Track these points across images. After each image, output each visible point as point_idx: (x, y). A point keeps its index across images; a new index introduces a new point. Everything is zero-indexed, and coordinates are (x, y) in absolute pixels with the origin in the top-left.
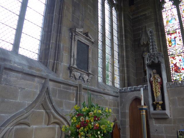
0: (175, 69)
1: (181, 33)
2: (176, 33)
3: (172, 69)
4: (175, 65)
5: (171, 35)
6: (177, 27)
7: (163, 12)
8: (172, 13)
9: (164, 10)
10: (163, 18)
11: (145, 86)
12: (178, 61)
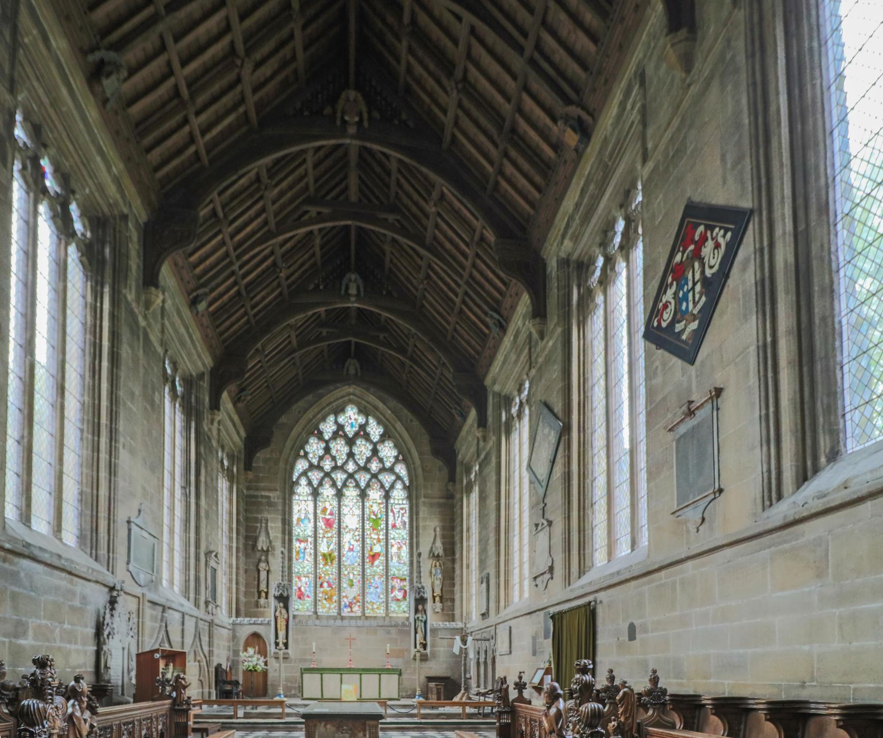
2: (307, 541)
4: (300, 589)
6: (310, 534)
9: (297, 497)
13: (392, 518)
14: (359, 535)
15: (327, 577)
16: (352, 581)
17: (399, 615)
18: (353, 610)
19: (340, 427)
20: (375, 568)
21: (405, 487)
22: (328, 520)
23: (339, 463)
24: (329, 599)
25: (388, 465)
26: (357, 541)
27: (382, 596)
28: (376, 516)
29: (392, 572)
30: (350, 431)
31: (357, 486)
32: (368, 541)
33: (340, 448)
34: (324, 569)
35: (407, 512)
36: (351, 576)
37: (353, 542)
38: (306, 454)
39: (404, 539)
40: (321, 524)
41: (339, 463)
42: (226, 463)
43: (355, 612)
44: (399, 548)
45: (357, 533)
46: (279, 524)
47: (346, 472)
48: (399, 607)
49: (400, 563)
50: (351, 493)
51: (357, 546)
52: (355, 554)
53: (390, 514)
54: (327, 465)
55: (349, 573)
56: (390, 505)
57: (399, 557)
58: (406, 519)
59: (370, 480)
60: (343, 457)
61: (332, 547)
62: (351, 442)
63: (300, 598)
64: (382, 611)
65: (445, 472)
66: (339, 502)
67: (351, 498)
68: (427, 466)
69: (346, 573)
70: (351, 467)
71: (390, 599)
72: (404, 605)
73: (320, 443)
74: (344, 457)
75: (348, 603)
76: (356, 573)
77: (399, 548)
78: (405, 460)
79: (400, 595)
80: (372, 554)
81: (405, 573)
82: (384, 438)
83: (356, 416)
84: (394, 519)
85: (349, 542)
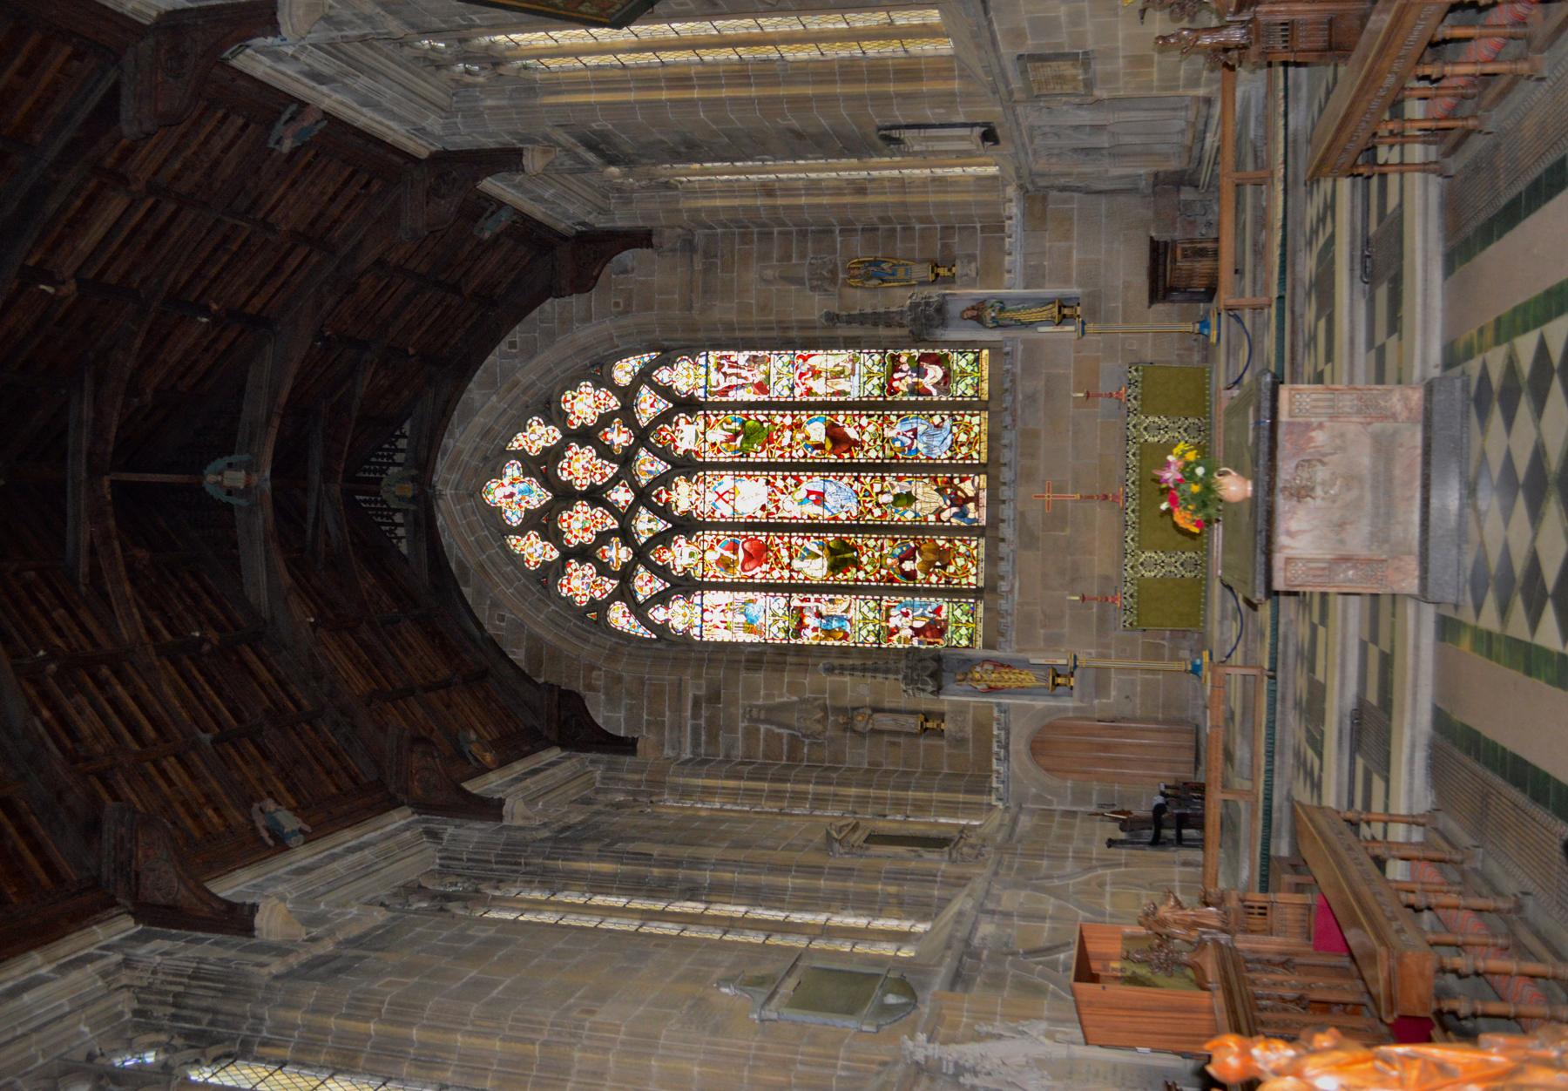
0: (933, 637)
1: (809, 596)
3: (929, 643)
5: (807, 627)
6: (783, 601)
7: (701, 636)
8: (720, 608)
9: (696, 631)
10: (726, 640)
11: (1000, 711)
12: (906, 622)
13: (741, 392)
14: (784, 478)
15: (889, 561)
16: (897, 497)
17: (986, 374)
18: (971, 494)
20: (866, 437)
21: (667, 360)
22: (747, 554)
23: (612, 523)
24: (945, 557)
25: (614, 403)
26: (798, 483)
27: (937, 420)
28: (737, 434)
29: (876, 392)
30: (538, 497)
31: (665, 480)
32: (798, 454)
33: (580, 523)
34: (869, 568)
35: (725, 353)
36: (884, 499)
37: (801, 494)
39: (792, 363)
40: (759, 573)
41: (612, 523)
42: (620, 798)
43: (978, 489)
44: (816, 374)
45: (780, 483)
46: (760, 677)
47: (633, 509)
48: (963, 372)
49: (853, 373)
50: (683, 496)
51: (815, 483)
52: (831, 488)
53: (733, 396)
54: (618, 554)
55: (878, 505)
56: (710, 399)
57: (838, 375)
58: (742, 357)
60: (599, 515)
61: (814, 548)
62: (565, 496)
63: (941, 633)
64: (976, 420)
65: (627, 257)
66: (705, 526)
67: (695, 496)
68: (617, 304)
69: (877, 512)
70: (622, 496)
71: (944, 399)
72: (960, 362)
73: (569, 570)
74: (598, 511)
75: (955, 510)
76: (877, 488)
77: (816, 374)
79: (935, 373)
80: (829, 446)
81: (877, 358)
82: (553, 413)
83: (506, 481)
84: (743, 386)
85: (801, 503)
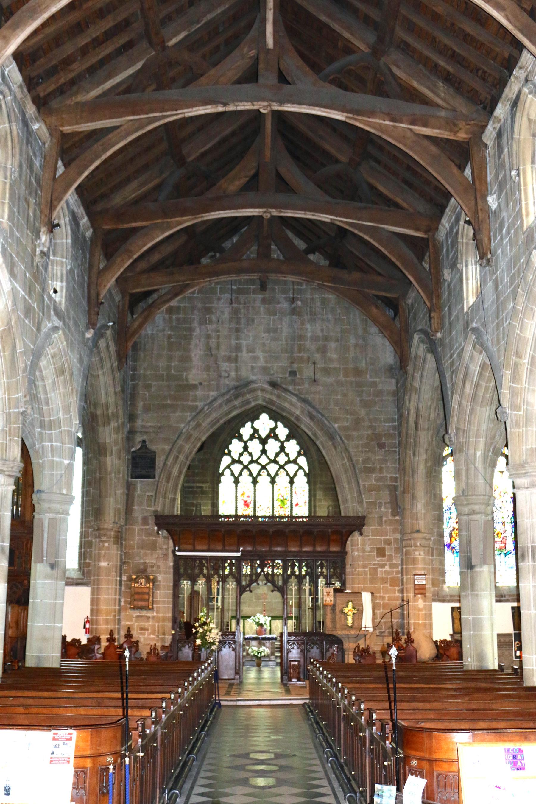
19: (256, 431)
21: (306, 475)
33: (255, 446)
38: (230, 452)
47: (259, 464)
50: (264, 480)
54: (246, 459)
59: (279, 470)
62: (263, 442)
78: (305, 455)
82: (288, 438)
